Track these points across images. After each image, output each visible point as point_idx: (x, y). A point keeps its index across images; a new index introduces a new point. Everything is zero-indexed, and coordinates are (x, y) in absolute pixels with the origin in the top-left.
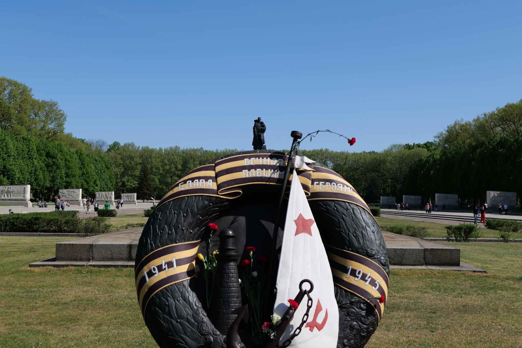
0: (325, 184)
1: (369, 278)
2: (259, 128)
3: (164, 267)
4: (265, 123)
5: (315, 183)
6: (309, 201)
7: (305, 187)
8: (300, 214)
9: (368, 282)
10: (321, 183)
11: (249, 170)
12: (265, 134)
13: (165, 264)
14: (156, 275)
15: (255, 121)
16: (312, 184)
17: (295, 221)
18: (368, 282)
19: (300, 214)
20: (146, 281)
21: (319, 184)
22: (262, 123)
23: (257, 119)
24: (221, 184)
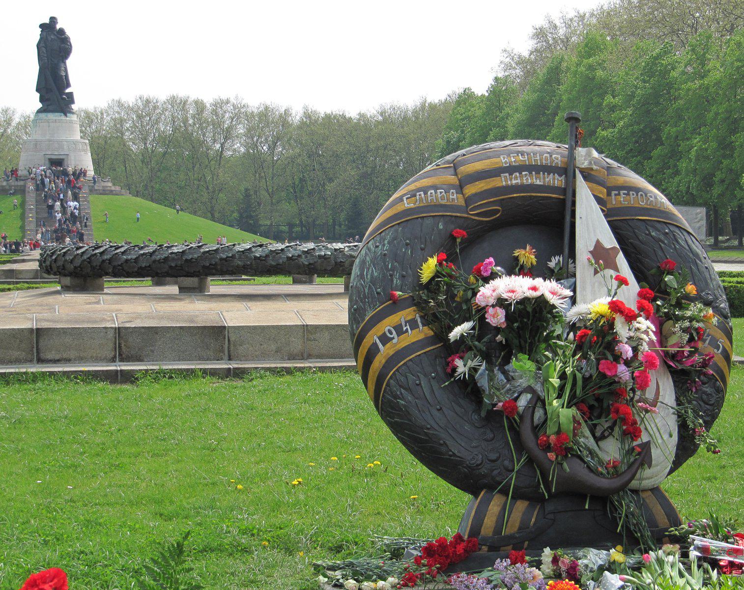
0: (628, 194)
1: (708, 335)
2: (54, 46)
3: (405, 329)
4: (68, 33)
5: (613, 193)
6: (609, 222)
7: (599, 201)
8: (598, 242)
9: (707, 342)
10: (622, 192)
11: (511, 174)
12: (71, 63)
13: (406, 322)
14: (394, 341)
16: (609, 194)
17: (590, 252)
18: (707, 342)
19: (598, 242)
20: (379, 351)
21: (619, 194)
22: (62, 31)
23: (47, 21)
24: (469, 196)
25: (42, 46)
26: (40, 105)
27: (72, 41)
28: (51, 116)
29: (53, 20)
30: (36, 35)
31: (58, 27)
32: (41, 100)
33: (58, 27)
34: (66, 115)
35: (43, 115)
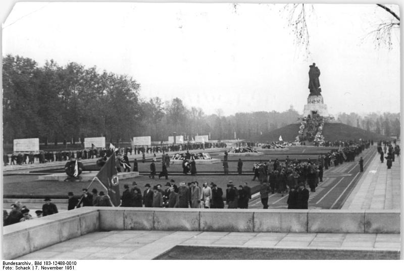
2: (314, 73)
4: (319, 68)
12: (320, 78)
15: (310, 66)
22: (317, 68)
23: (312, 64)
25: (310, 73)
26: (309, 93)
27: (320, 71)
29: (314, 64)
30: (309, 69)
31: (316, 66)
32: (311, 91)
33: (316, 66)
35: (311, 97)
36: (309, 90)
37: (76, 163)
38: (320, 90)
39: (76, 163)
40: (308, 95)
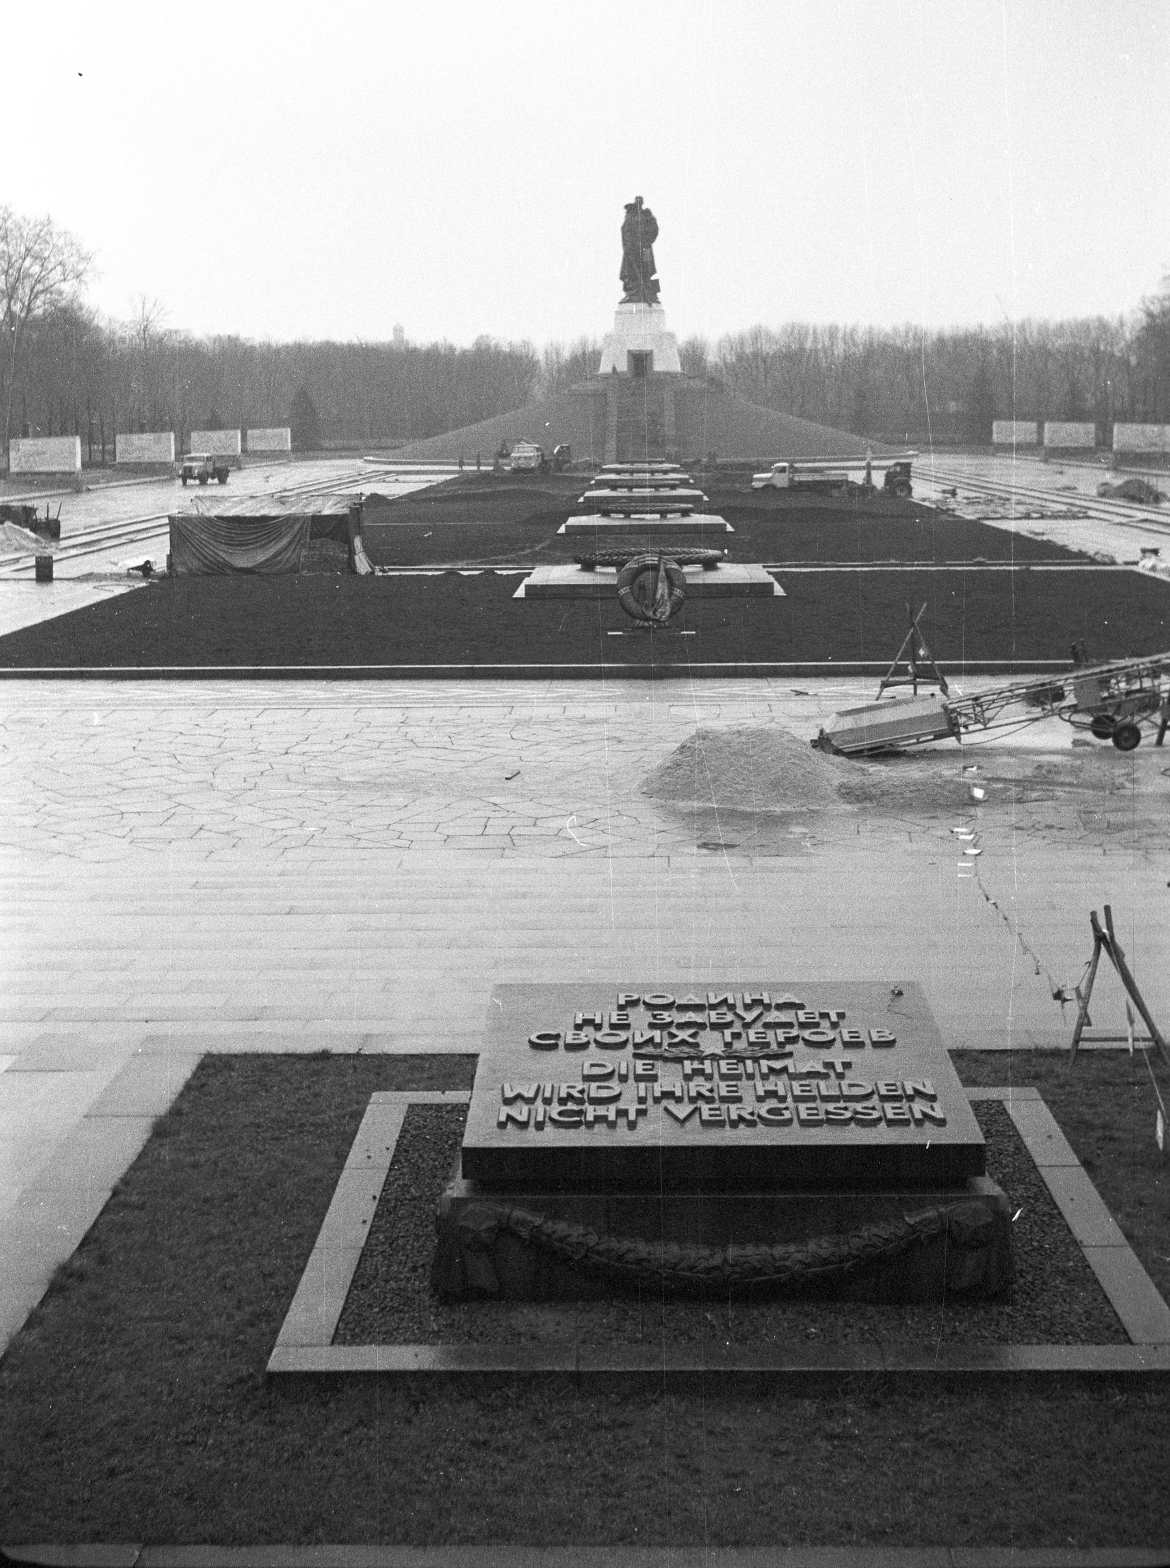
2: (640, 228)
4: (655, 214)
12: (657, 247)
15: (628, 207)
22: (648, 212)
23: (632, 201)
26: (623, 295)
27: (659, 223)
28: (633, 307)
29: (640, 200)
30: (621, 217)
31: (644, 207)
32: (625, 289)
33: (644, 207)
34: (650, 305)
36: (621, 284)
37: (662, 573)
38: (656, 286)
39: (662, 573)
40: (615, 306)
